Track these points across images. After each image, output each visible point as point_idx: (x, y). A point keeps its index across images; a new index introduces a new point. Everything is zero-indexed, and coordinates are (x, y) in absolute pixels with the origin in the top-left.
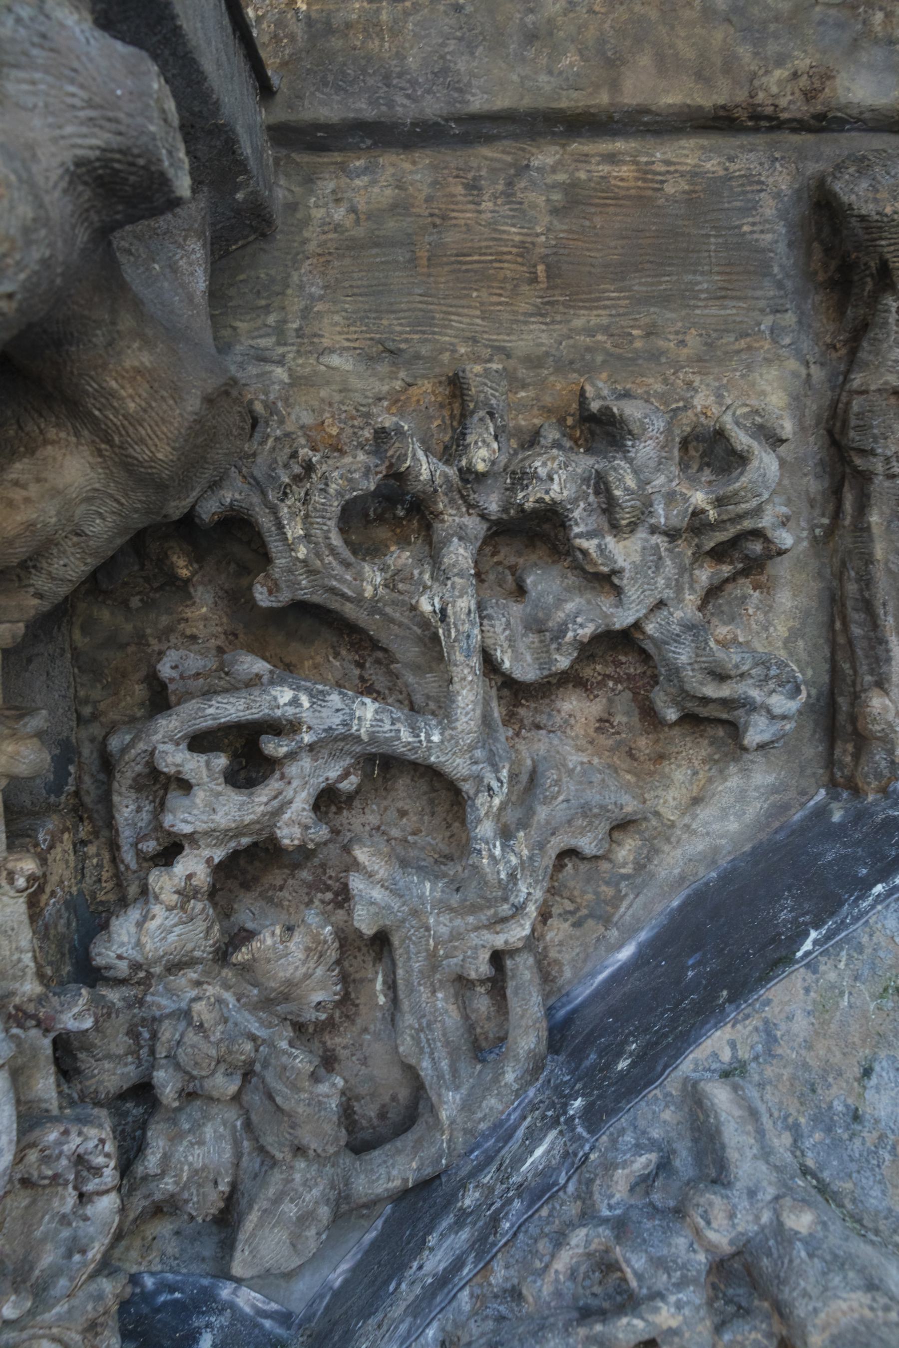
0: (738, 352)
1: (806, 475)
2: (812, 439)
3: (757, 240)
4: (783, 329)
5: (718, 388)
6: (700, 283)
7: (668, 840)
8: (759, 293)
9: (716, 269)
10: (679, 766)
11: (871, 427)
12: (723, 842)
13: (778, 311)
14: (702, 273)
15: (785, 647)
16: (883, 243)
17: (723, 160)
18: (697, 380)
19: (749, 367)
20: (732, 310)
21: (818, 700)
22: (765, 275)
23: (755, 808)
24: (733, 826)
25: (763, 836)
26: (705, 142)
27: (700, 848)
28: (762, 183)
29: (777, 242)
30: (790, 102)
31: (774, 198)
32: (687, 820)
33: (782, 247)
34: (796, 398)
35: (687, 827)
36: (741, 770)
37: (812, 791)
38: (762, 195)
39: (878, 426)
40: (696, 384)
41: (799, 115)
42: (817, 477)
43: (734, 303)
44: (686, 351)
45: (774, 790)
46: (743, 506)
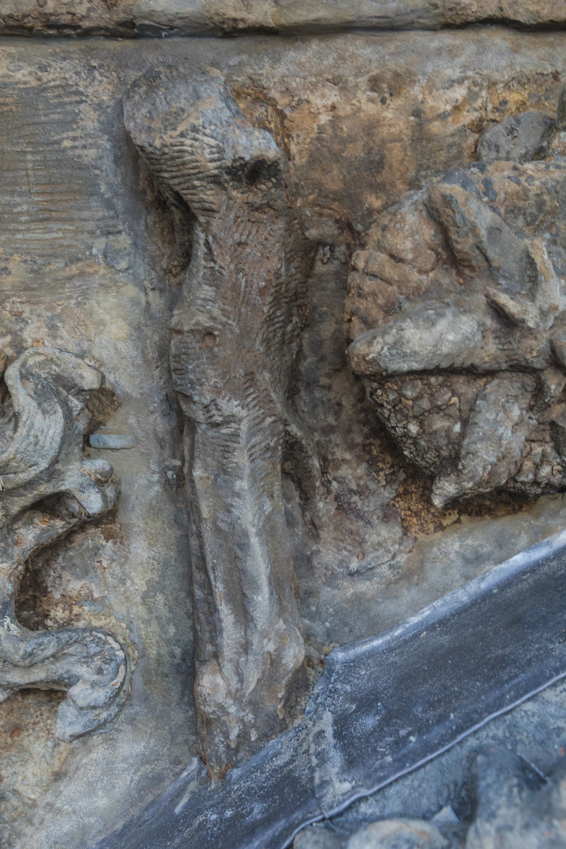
0: (70, 279)
1: (152, 413)
2: (156, 373)
3: (79, 157)
4: (118, 252)
5: (52, 319)
6: (18, 204)
7: (30, 821)
8: (86, 214)
9: (35, 189)
10: (38, 738)
11: (187, 372)
12: (92, 820)
13: (109, 233)
14: (21, 194)
15: (144, 603)
16: (166, 175)
17: (34, 69)
18: (26, 310)
19: (84, 294)
20: (57, 233)
21: (184, 660)
22: (92, 194)
23: (125, 782)
24: (102, 802)
25: (135, 812)
26: (13, 50)
27: (67, 828)
28: (81, 93)
29: (101, 158)
30: (89, 10)
31: (95, 110)
32: (49, 798)
33: (107, 164)
34: (138, 328)
35: (50, 806)
36: (105, 740)
37: (185, 759)
38: (82, 106)
39: (193, 371)
40: (25, 315)
41: (102, 24)
42: (165, 415)
43: (60, 225)
44: (10, 279)
45: (145, 760)
46: (21, 476)
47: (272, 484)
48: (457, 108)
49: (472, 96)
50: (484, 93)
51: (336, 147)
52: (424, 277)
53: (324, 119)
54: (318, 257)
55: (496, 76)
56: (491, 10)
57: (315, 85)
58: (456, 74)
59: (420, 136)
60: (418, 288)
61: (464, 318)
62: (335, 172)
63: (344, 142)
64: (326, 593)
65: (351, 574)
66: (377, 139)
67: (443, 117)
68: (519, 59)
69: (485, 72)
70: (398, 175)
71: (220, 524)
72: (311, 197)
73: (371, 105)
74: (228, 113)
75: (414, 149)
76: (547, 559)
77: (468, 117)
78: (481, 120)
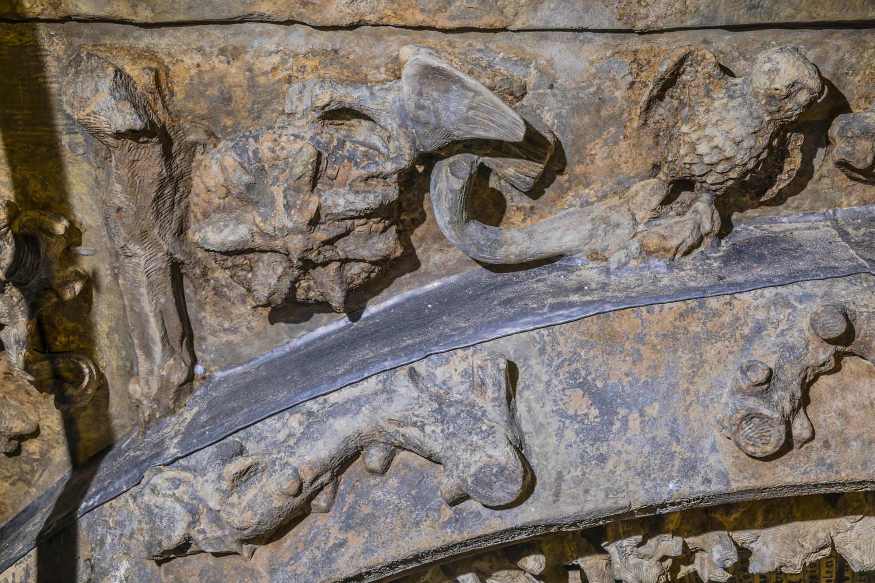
47: (165, 287)
48: (274, 69)
49: (284, 61)
50: (291, 60)
51: (201, 88)
52: (222, 201)
53: (193, 71)
54: (197, 150)
55: (299, 50)
56: (285, 17)
57: (186, 51)
58: (273, 48)
59: (252, 85)
60: (218, 207)
61: (241, 227)
62: (203, 103)
63: (205, 85)
64: (211, 339)
65: (224, 330)
66: (226, 85)
67: (265, 73)
68: (312, 40)
69: (291, 48)
70: (241, 106)
71: (135, 308)
72: (189, 117)
73: (221, 65)
74: (113, 102)
75: (250, 92)
76: (334, 333)
77: (281, 74)
78: (290, 76)
